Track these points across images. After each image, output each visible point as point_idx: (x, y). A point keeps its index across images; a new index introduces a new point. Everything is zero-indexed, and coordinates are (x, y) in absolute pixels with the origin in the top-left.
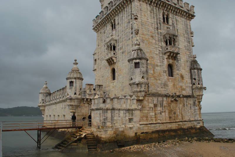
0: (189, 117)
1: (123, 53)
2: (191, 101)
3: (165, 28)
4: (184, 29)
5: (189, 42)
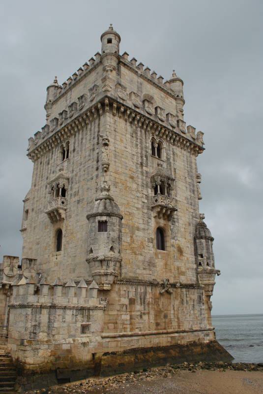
0: (191, 323)
2: (194, 295)
3: (155, 165)
5: (194, 191)
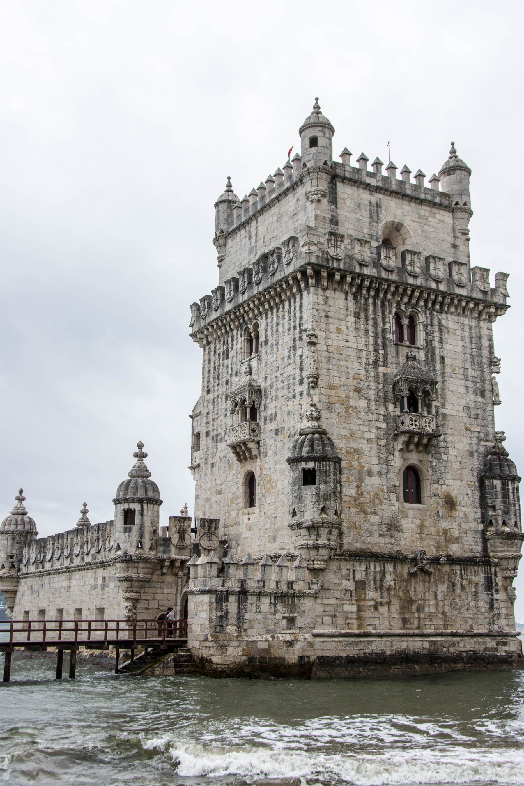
0: (470, 622)
3: (402, 360)
4: (468, 351)
5: (482, 394)
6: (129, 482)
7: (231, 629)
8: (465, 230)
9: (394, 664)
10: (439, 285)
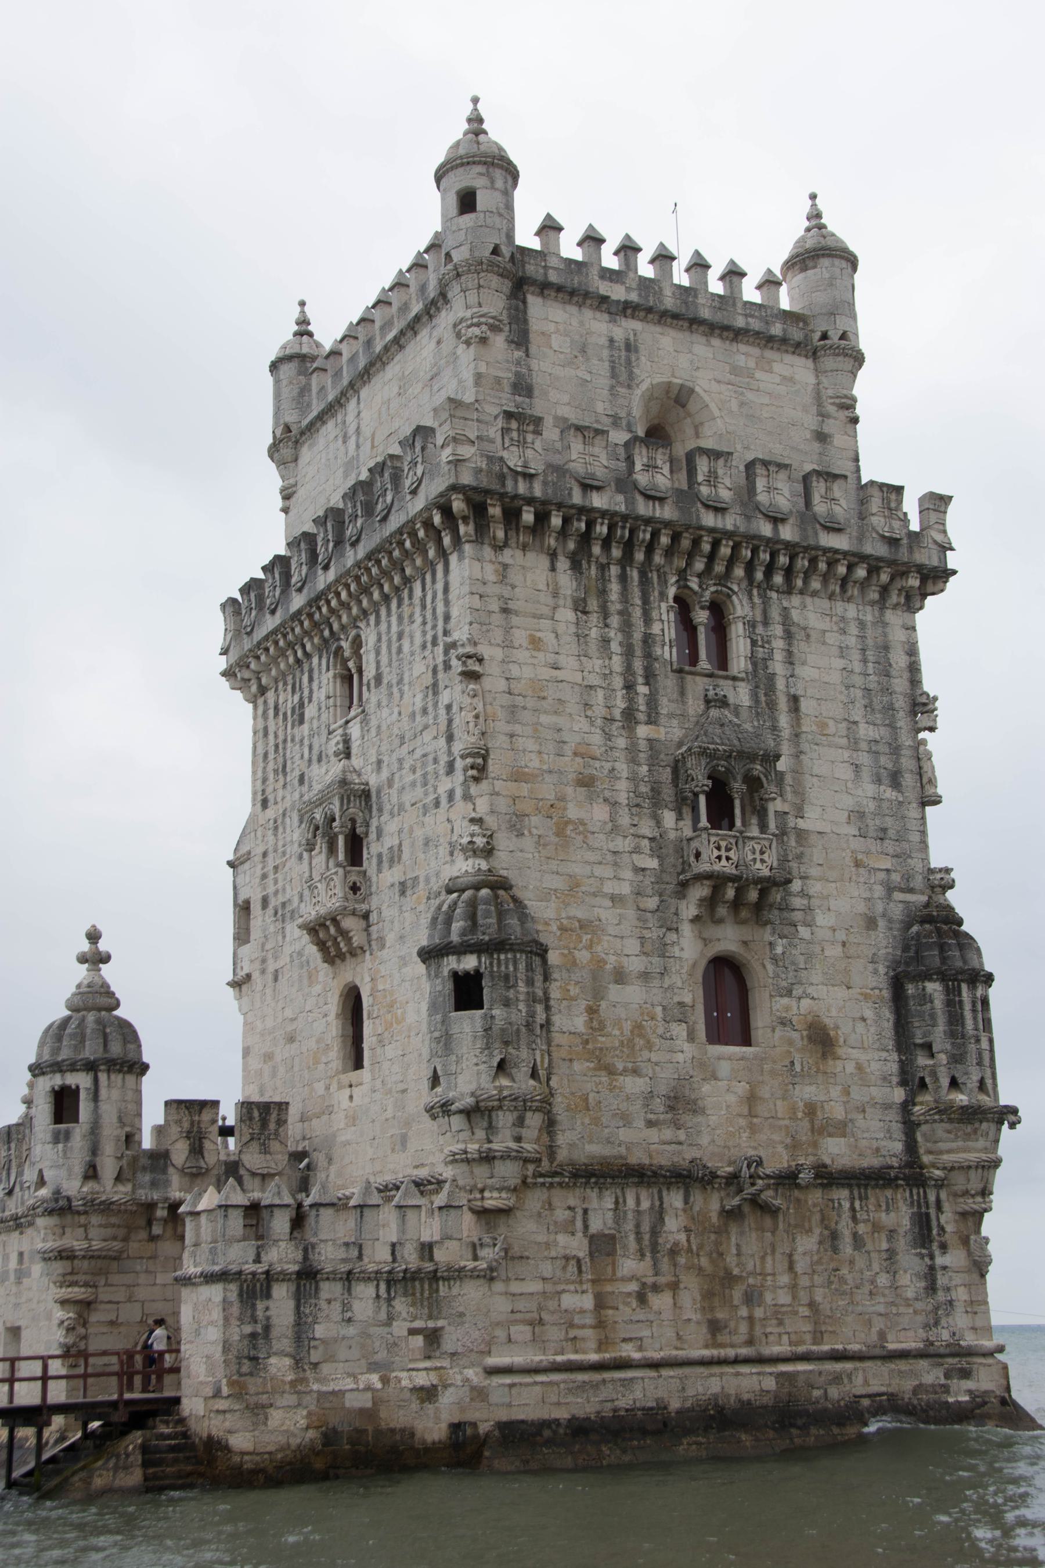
0: (878, 1324)
1: (403, 893)
3: (694, 706)
4: (858, 680)
6: (66, 1021)
7: (279, 1366)
8: (846, 397)
9: (688, 1432)
10: (780, 527)
